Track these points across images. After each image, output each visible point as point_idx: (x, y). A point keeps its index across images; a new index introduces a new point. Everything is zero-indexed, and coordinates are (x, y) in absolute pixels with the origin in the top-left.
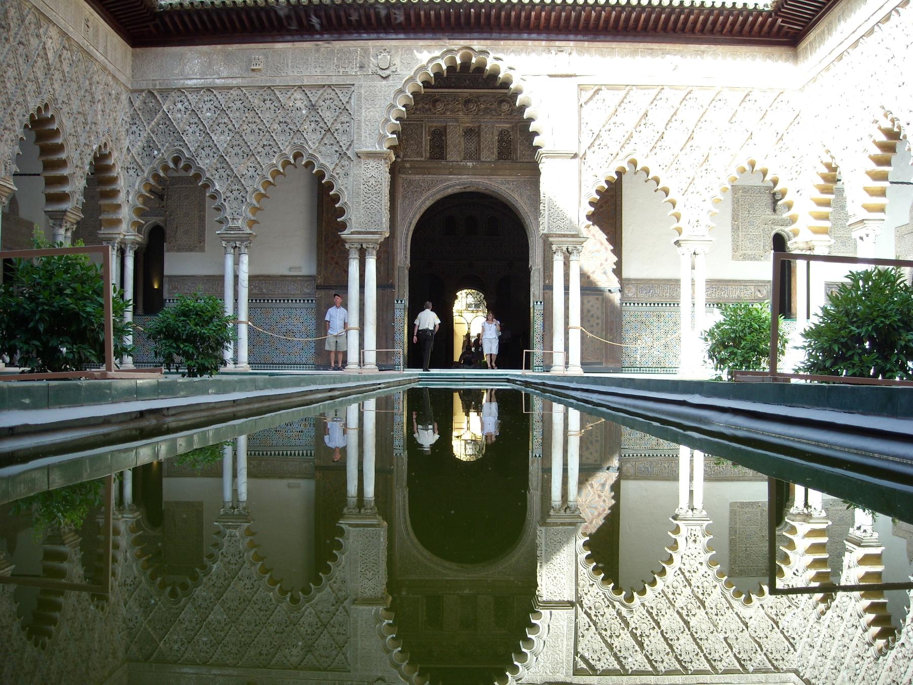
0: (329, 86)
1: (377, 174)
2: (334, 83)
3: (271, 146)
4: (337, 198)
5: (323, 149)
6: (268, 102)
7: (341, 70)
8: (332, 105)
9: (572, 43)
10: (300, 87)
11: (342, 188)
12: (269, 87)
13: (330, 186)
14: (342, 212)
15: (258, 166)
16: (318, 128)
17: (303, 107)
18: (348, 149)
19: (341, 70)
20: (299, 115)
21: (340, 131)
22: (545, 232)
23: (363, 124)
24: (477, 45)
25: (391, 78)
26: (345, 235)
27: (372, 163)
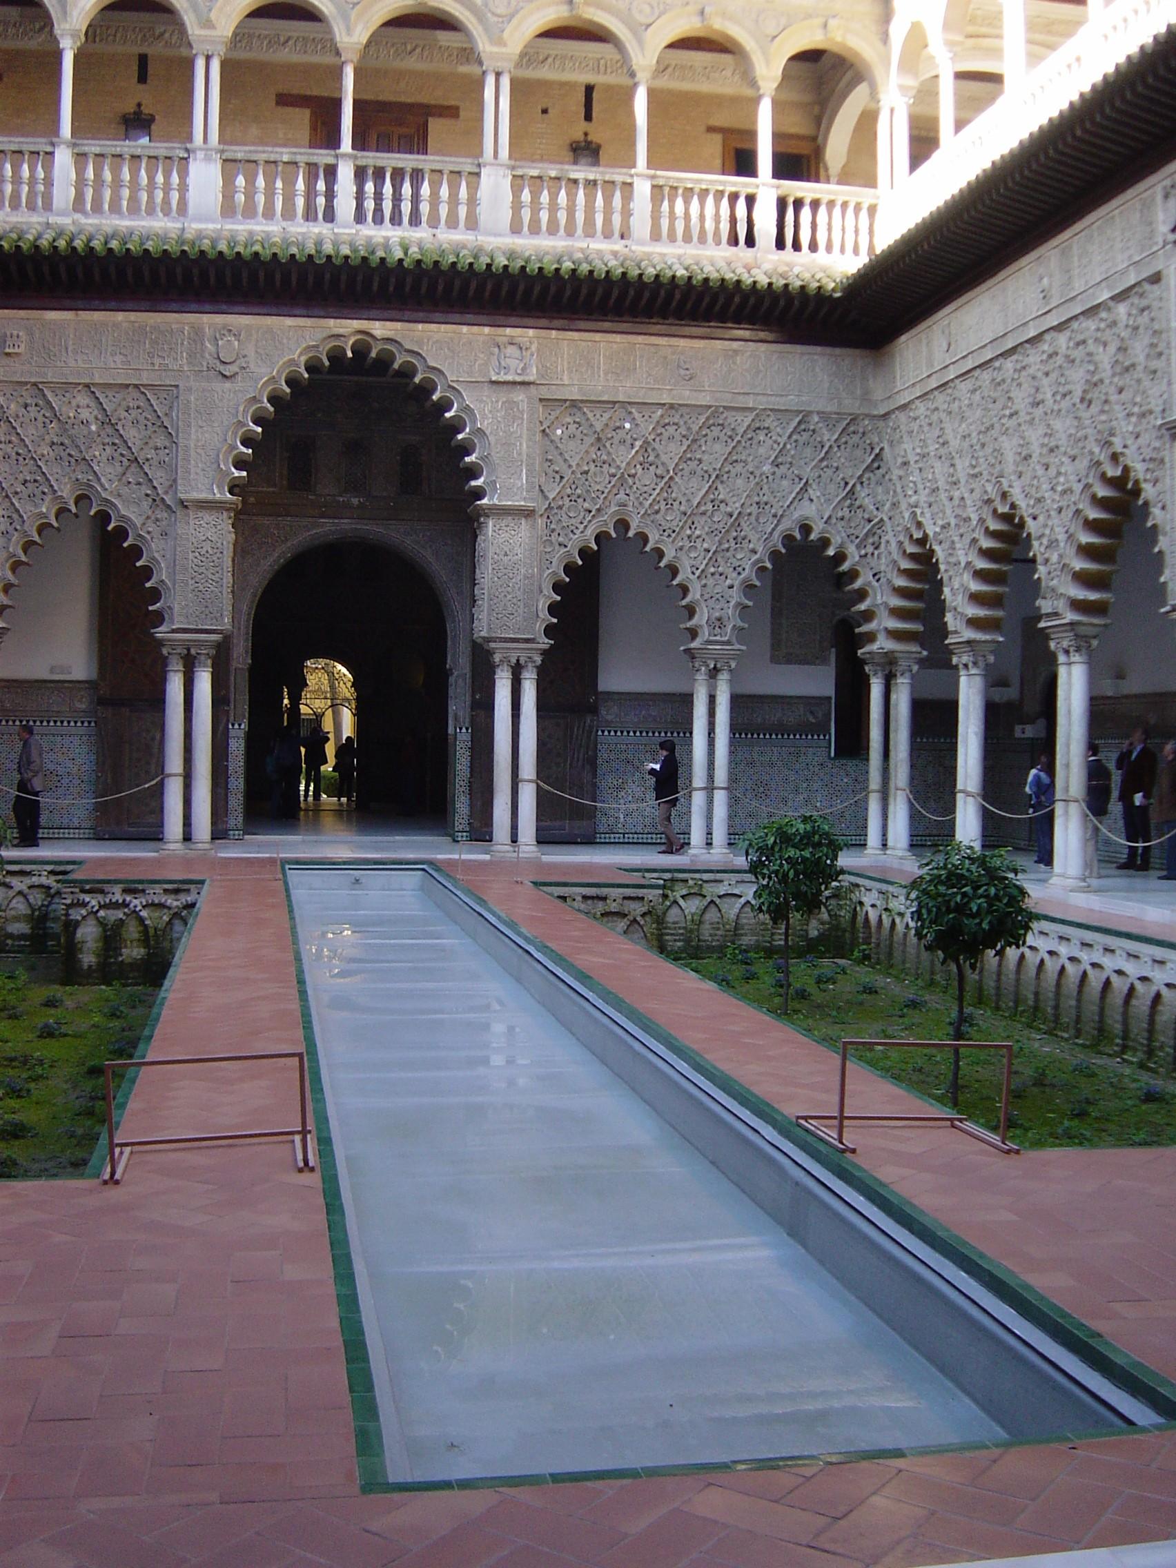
0: (136, 386)
1: (213, 536)
2: (145, 382)
3: (40, 483)
4: (147, 572)
5: (125, 491)
6: (32, 409)
7: (157, 361)
8: (141, 418)
9: (531, 332)
10: (87, 386)
11: (156, 555)
12: (35, 384)
13: (137, 552)
14: (155, 595)
15: (15, 516)
16: (116, 455)
17: (91, 419)
18: (166, 493)
19: (157, 361)
20: (85, 432)
21: (154, 462)
22: (483, 634)
23: (192, 453)
24: (380, 329)
25: (239, 378)
26: (161, 632)
27: (208, 517)
